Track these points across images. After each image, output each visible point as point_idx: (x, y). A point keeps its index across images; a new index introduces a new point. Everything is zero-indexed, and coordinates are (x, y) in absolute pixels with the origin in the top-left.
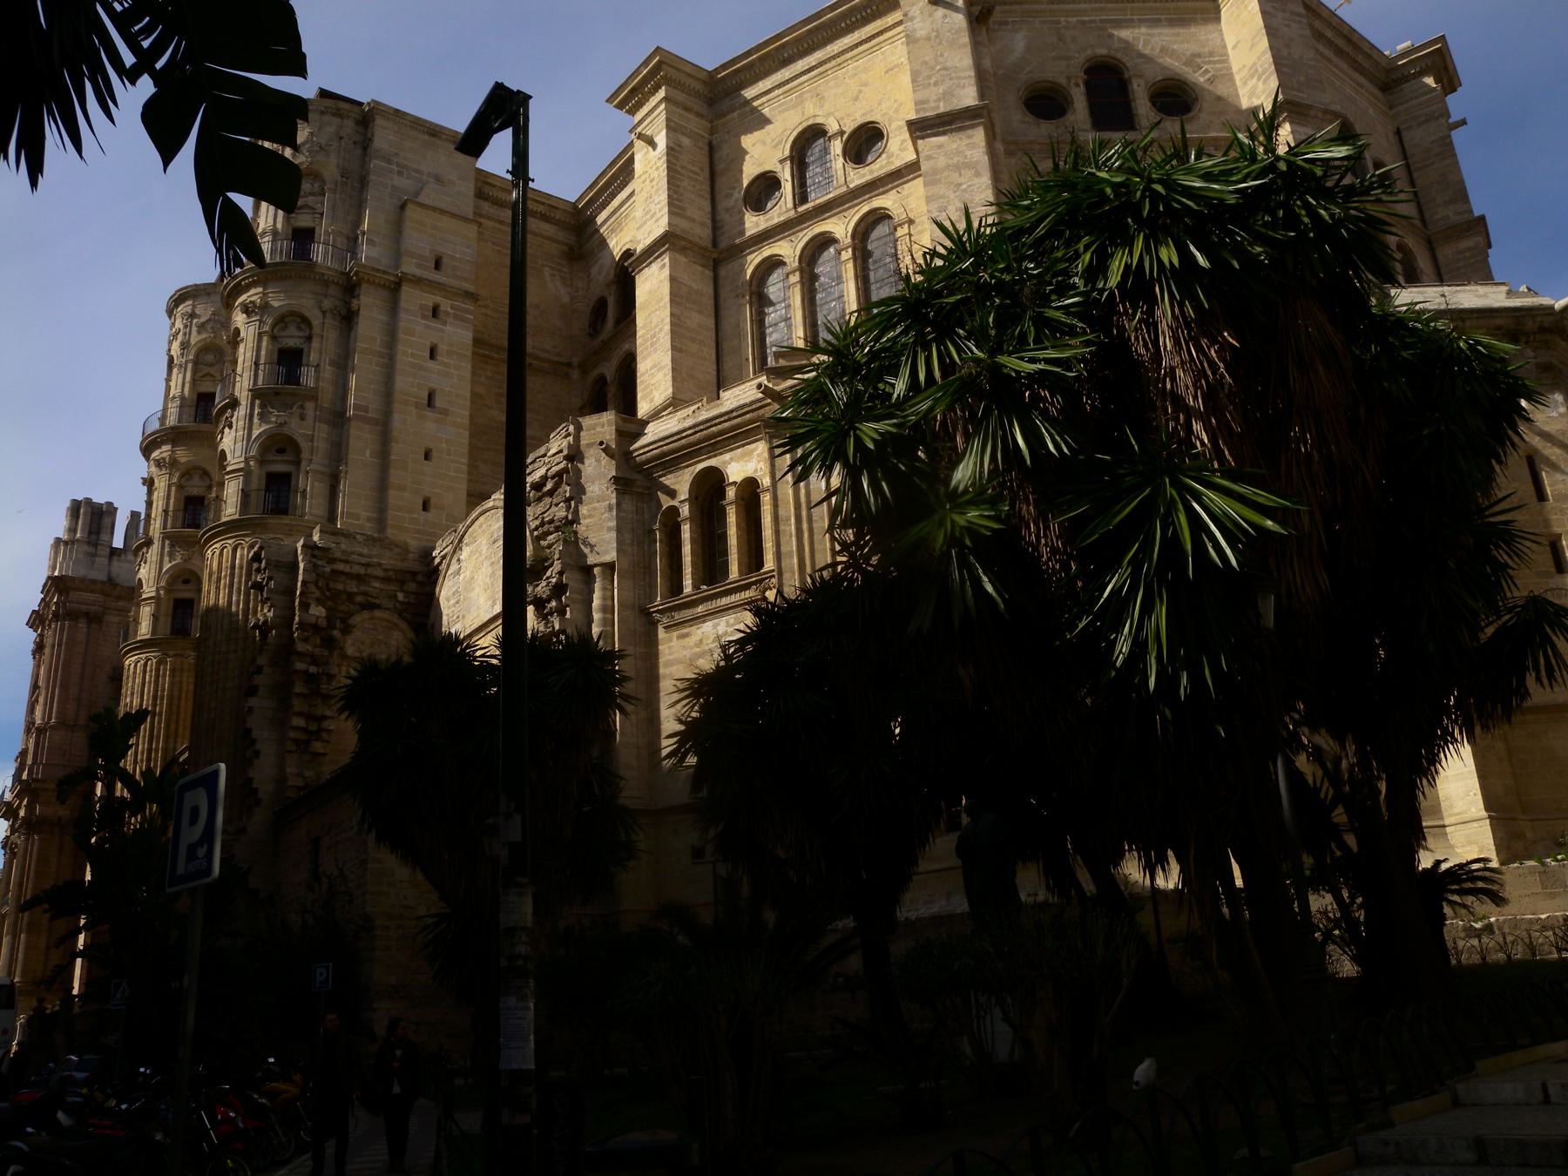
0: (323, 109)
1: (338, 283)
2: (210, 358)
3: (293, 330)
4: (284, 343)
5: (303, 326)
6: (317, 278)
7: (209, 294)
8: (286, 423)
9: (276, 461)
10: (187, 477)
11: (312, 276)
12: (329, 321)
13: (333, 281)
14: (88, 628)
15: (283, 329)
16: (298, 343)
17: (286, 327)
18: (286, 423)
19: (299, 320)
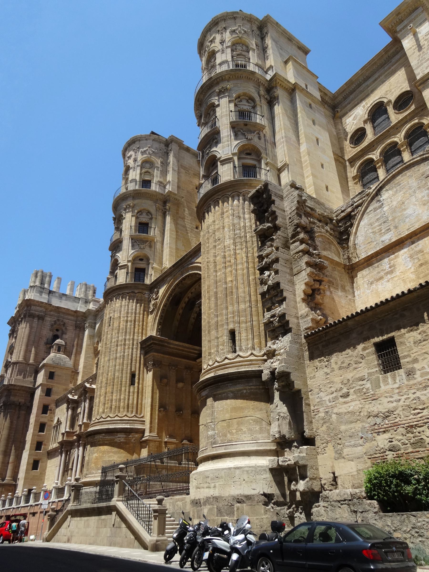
1: (264, 85)
2: (148, 165)
3: (244, 102)
5: (250, 101)
6: (255, 80)
7: (146, 140)
8: (252, 139)
9: (247, 158)
10: (140, 213)
11: (253, 79)
12: (263, 101)
13: (262, 84)
14: (38, 322)
15: (239, 102)
16: (249, 109)
17: (241, 101)
18: (252, 139)
19: (247, 98)
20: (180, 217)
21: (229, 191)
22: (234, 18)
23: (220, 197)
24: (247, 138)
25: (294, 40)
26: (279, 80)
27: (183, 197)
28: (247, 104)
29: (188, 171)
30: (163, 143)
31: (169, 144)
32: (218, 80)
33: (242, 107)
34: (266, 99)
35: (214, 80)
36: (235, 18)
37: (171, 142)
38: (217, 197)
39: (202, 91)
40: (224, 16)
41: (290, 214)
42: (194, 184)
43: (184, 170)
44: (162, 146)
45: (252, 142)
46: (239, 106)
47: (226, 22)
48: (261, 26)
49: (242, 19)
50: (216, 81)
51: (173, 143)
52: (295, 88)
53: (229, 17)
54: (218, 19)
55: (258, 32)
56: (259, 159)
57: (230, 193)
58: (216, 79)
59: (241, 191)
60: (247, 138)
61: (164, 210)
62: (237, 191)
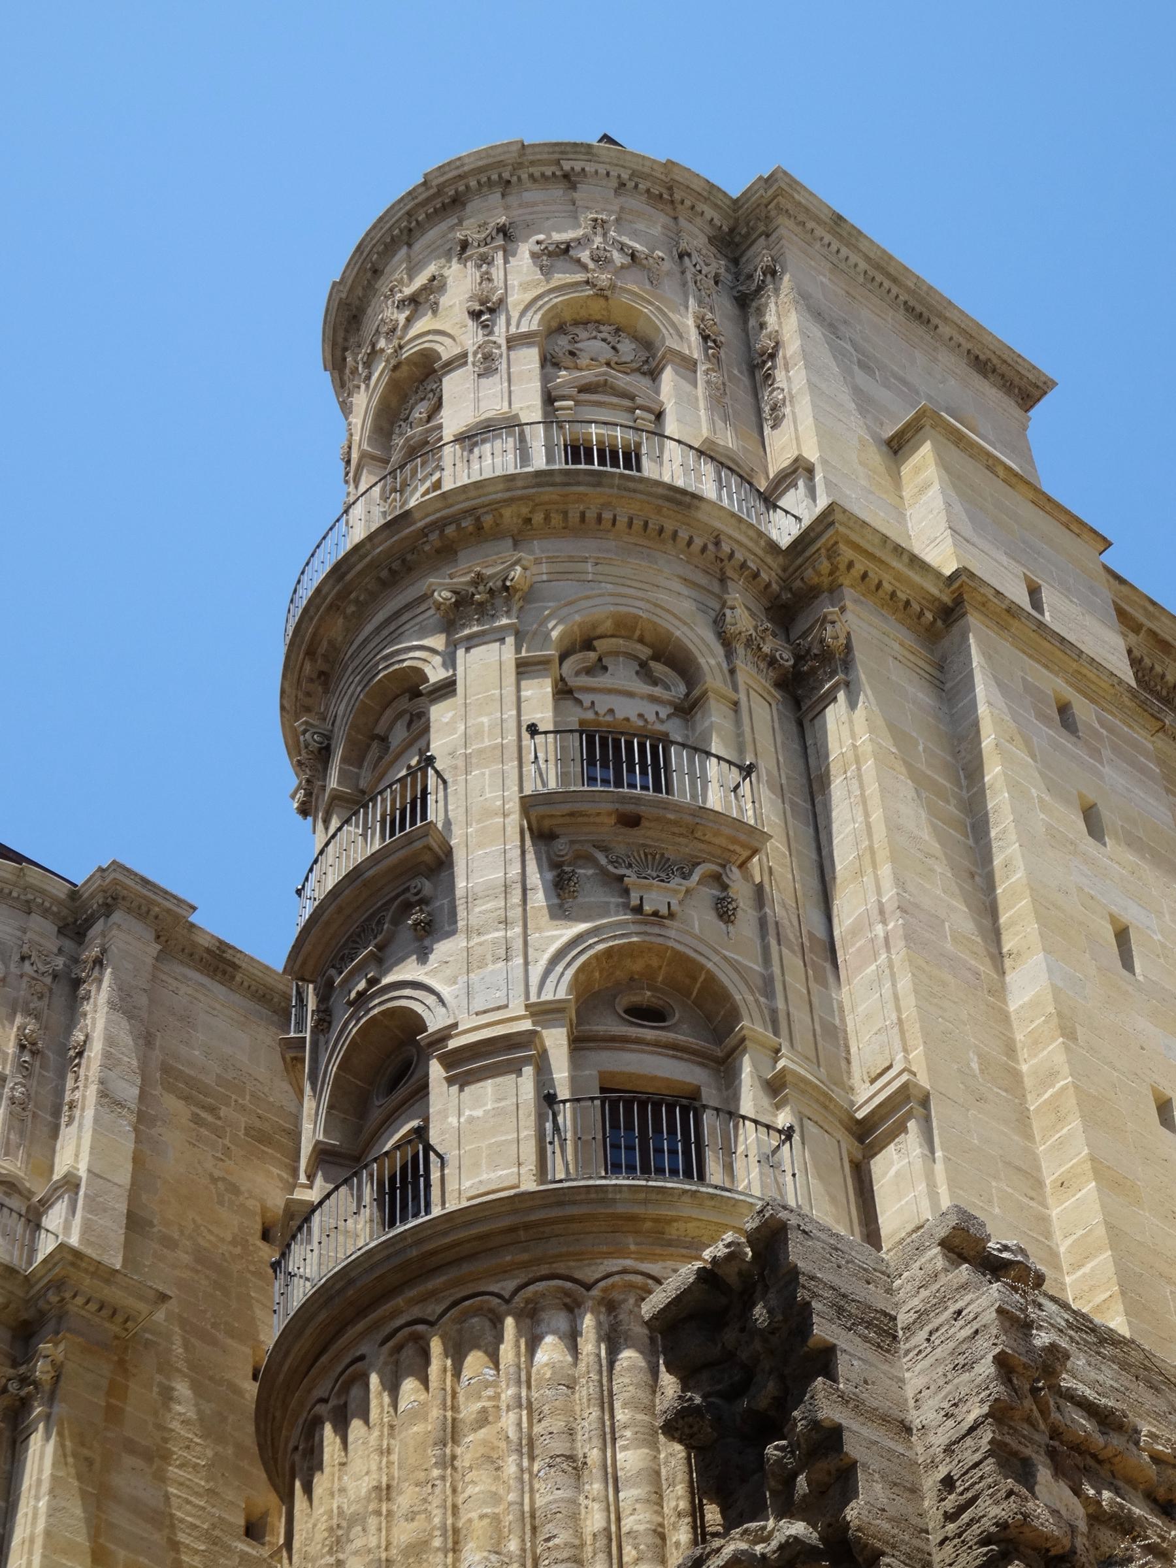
0: (625, 176)
1: (756, 575)
3: (622, 676)
4: (602, 708)
5: (658, 668)
6: (698, 542)
8: (671, 915)
9: (638, 1041)
11: (683, 535)
12: (749, 674)
13: (743, 565)
15: (589, 671)
16: (651, 718)
17: (600, 667)
18: (671, 915)
19: (644, 652)
20: (131, 1447)
21: (504, 1272)
22: (566, 176)
23: (433, 1309)
24: (639, 910)
25: (946, 320)
26: (856, 547)
27: (163, 1298)
28: (647, 689)
29: (213, 1110)
30: (45, 912)
31: (90, 922)
32: (450, 530)
33: (604, 703)
34: (772, 662)
35: (424, 532)
36: (569, 180)
37: (108, 909)
38: (416, 1312)
39: (343, 596)
40: (501, 164)
41: (948, 1450)
42: (252, 1204)
43: (187, 1099)
44: (43, 931)
45: (674, 937)
46: (587, 699)
47: (512, 200)
48: (732, 230)
49: (614, 183)
50: (434, 537)
51: (117, 916)
52: (959, 601)
53: (536, 171)
54: (461, 177)
55: (718, 265)
56: (719, 1053)
57: (507, 1286)
58: (439, 525)
59: (589, 1273)
60: (639, 910)
61: (13, 1387)
62: (560, 1268)
